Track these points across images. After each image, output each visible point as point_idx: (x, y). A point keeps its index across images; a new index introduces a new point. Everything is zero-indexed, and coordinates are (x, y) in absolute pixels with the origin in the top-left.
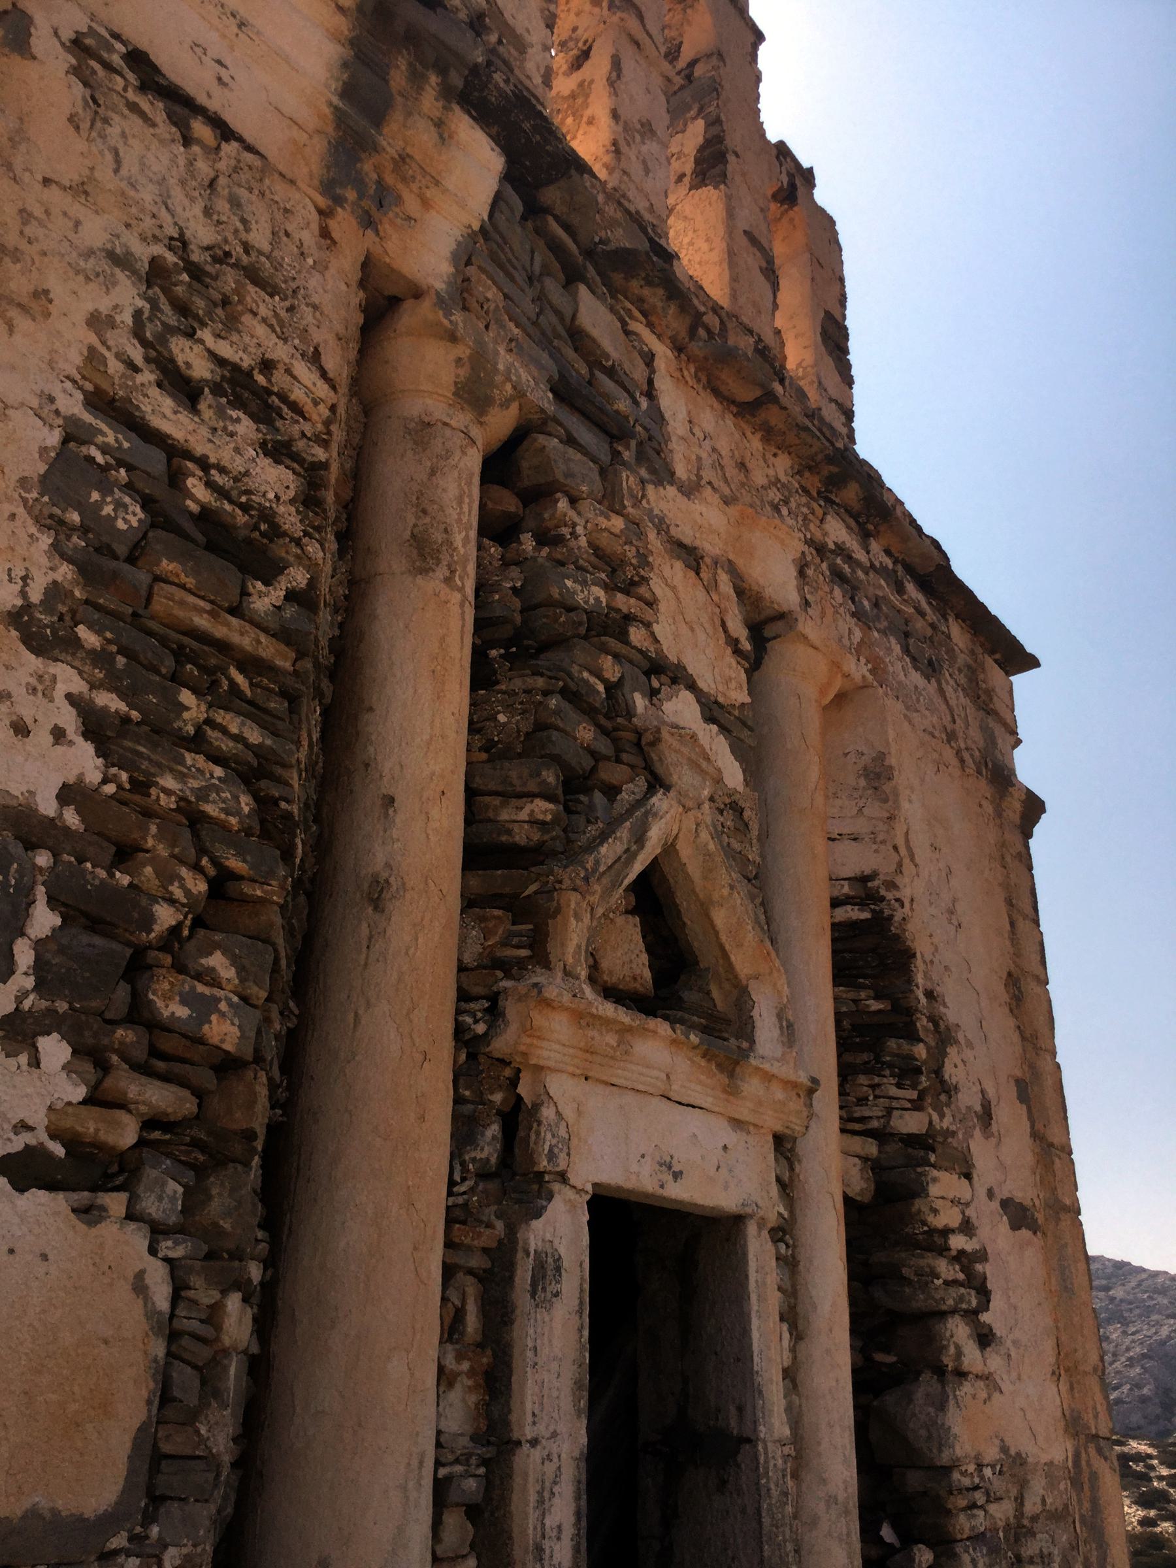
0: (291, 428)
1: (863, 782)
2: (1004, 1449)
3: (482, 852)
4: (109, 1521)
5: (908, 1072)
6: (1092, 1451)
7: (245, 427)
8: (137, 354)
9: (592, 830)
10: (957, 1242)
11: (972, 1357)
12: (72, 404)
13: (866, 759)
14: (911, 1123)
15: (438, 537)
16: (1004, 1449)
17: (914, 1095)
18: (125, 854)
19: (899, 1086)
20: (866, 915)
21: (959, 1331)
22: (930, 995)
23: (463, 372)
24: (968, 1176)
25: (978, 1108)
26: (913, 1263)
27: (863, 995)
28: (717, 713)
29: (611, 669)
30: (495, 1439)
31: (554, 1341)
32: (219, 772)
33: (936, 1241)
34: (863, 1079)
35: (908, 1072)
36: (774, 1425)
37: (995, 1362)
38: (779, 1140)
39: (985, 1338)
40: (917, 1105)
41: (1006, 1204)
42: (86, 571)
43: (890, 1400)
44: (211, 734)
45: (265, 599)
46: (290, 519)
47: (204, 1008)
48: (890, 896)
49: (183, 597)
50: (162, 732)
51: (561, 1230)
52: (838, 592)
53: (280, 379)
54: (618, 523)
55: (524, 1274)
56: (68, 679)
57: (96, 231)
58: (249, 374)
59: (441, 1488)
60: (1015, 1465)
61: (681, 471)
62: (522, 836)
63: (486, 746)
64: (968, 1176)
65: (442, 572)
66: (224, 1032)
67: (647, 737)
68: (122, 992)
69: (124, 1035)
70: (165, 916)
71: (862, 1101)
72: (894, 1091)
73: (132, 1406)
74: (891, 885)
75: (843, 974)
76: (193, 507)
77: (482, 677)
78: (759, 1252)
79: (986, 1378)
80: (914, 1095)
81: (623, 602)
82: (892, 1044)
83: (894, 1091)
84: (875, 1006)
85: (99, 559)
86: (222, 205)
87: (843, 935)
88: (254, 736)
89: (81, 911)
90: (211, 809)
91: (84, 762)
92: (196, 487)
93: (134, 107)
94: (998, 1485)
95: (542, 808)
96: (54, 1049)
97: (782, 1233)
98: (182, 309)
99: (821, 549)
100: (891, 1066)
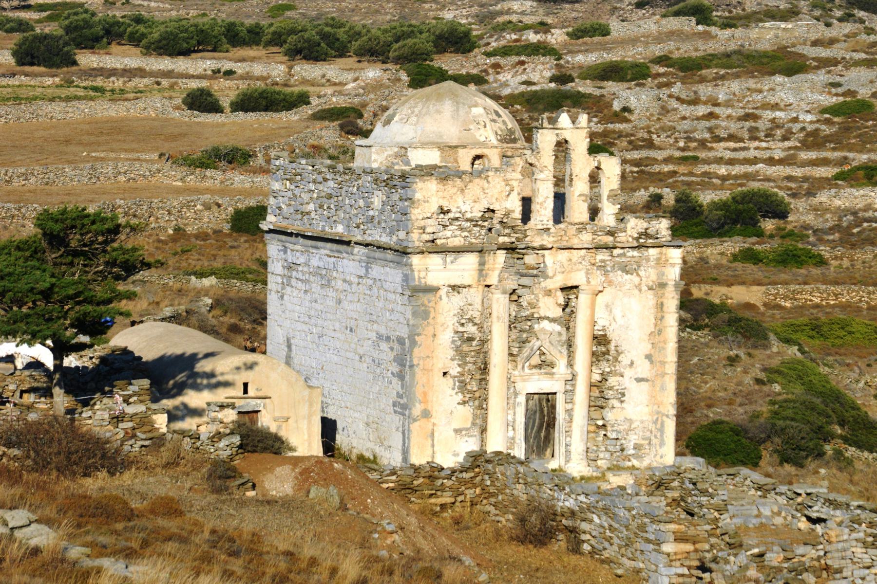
0: (477, 321)
3: (511, 355)
7: (471, 324)
12: (452, 335)
14: (608, 370)
29: (529, 323)
31: (521, 412)
33: (611, 388)
35: (608, 360)
37: (624, 405)
41: (636, 379)
42: (456, 351)
45: (474, 343)
46: (477, 332)
49: (465, 348)
50: (466, 363)
51: (522, 399)
52: (598, 272)
54: (533, 297)
56: (456, 362)
57: (452, 314)
59: (508, 425)
61: (550, 274)
62: (515, 353)
66: (475, 389)
73: (471, 419)
81: (533, 310)
85: (457, 349)
89: (461, 382)
91: (459, 369)
92: (466, 335)
99: (594, 264)
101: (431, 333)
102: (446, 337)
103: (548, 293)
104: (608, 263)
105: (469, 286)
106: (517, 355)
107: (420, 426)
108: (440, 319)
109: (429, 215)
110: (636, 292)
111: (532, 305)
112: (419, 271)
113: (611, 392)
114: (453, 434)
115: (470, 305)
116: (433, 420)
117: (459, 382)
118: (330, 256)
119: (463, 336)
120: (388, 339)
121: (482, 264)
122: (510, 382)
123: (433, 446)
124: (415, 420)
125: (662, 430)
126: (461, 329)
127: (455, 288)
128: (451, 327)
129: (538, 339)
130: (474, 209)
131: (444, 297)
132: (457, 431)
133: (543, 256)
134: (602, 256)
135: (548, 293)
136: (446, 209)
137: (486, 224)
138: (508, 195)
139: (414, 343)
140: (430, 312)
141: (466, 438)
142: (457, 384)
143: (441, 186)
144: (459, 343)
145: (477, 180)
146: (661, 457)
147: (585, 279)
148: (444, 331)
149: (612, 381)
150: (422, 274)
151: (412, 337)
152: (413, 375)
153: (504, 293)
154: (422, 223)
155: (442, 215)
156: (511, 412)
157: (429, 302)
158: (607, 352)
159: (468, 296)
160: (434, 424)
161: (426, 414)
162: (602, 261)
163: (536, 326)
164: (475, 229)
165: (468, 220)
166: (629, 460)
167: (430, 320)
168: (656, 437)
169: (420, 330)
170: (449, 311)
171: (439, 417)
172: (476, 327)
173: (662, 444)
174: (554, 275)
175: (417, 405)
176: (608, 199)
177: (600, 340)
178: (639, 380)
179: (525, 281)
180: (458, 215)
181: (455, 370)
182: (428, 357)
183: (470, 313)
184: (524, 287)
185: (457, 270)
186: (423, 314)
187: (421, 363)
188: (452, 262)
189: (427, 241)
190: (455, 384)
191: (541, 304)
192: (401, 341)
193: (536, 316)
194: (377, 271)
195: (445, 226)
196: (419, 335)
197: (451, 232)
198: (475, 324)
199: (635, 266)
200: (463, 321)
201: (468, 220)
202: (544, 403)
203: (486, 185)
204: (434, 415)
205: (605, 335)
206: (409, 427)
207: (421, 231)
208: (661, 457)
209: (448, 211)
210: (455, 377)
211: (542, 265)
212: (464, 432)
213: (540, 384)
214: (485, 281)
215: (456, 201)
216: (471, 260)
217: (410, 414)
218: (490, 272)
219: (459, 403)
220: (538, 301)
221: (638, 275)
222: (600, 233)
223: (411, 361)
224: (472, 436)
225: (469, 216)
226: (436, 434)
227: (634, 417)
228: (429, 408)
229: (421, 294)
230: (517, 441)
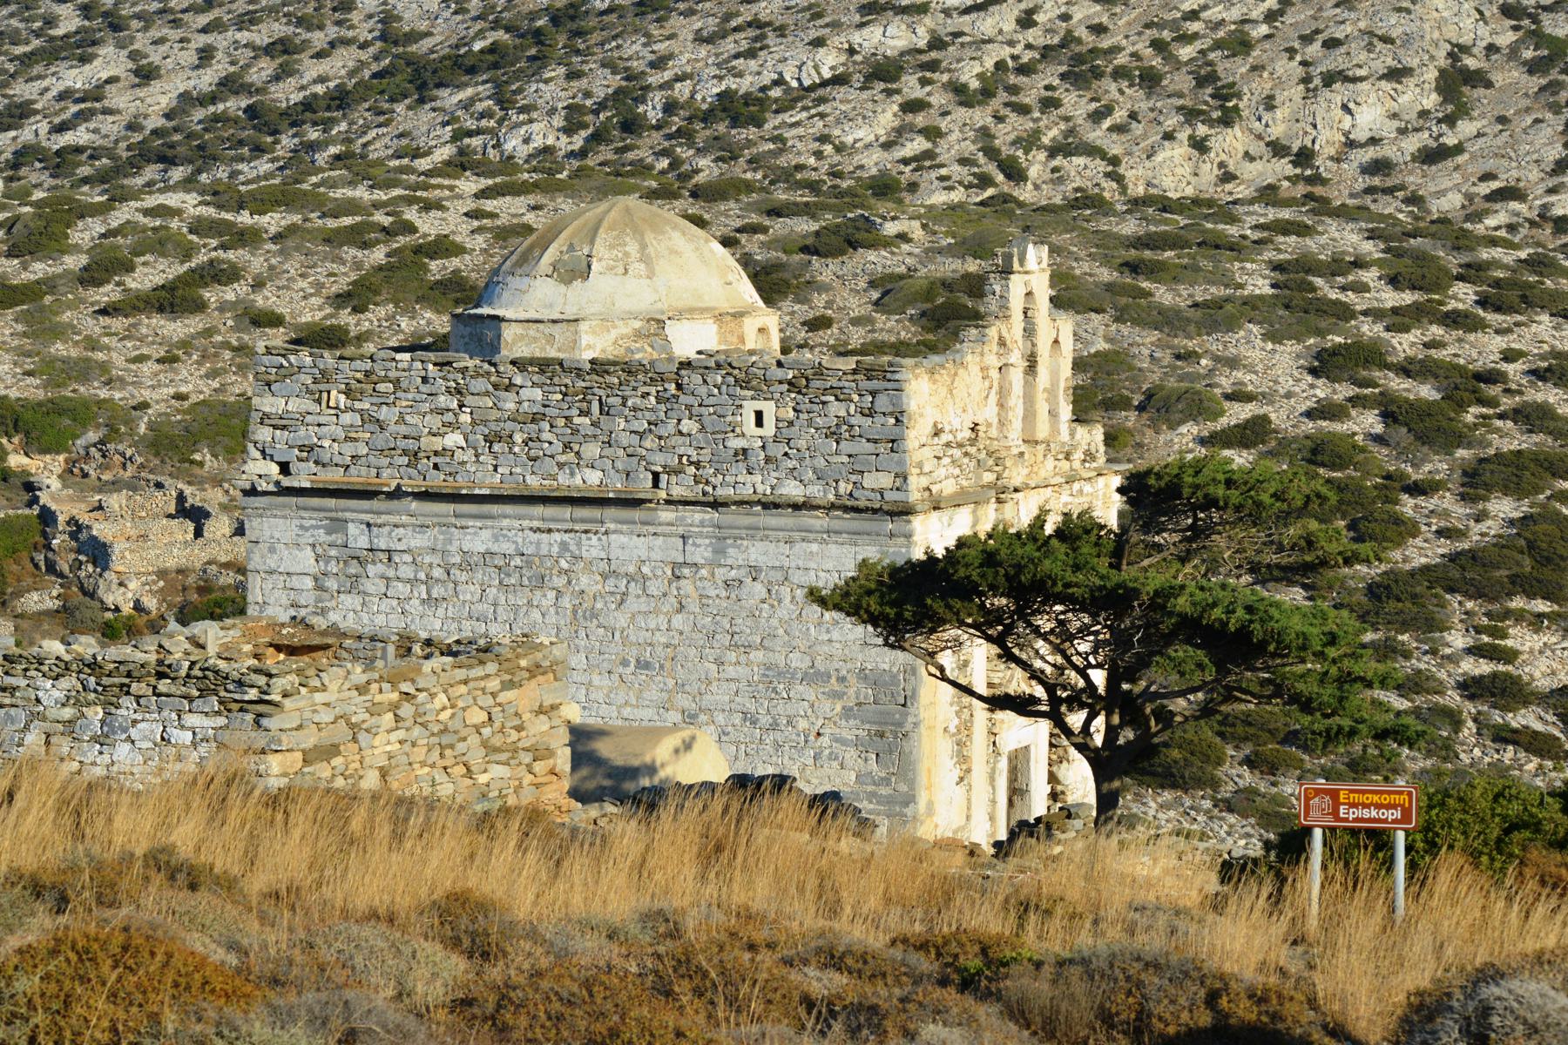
118: (550, 531)
194: (757, 553)
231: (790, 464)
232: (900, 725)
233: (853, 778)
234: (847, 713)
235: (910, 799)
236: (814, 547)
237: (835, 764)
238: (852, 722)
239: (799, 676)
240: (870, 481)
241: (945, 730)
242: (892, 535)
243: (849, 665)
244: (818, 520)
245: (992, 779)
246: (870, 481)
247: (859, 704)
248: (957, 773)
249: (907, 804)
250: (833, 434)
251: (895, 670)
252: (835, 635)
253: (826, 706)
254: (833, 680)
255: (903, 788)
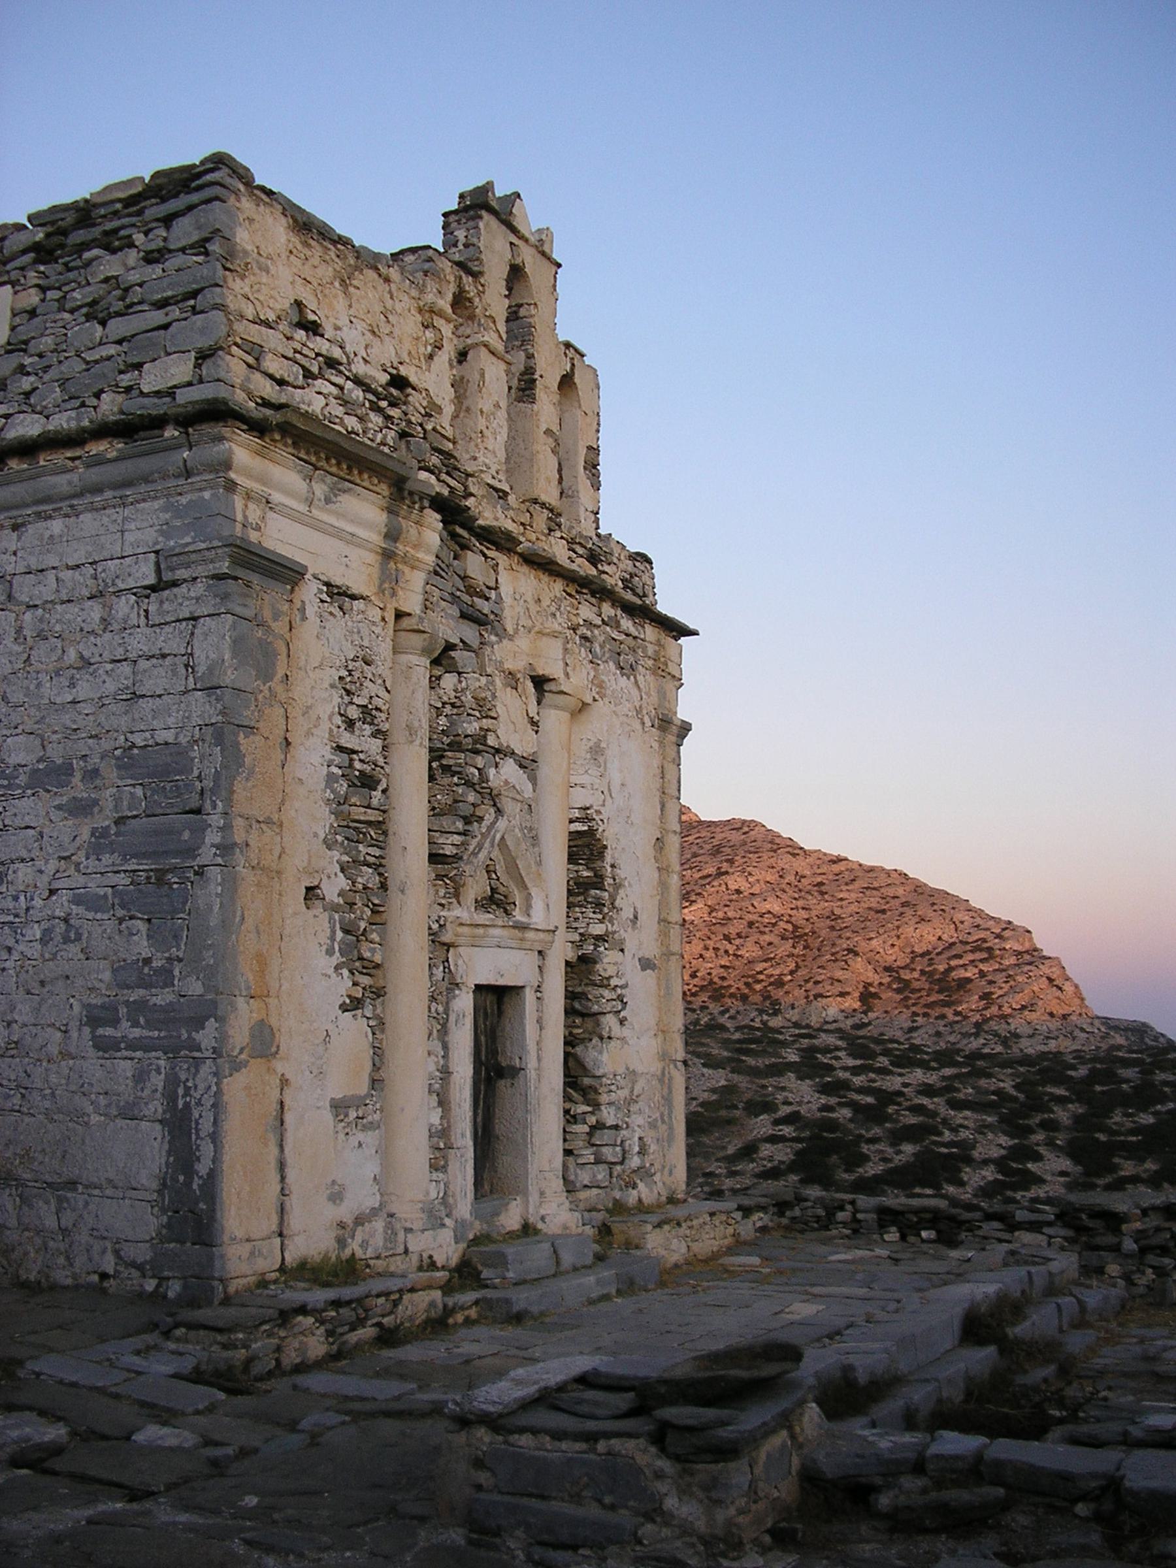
1: (588, 756)
2: (628, 1069)
3: (435, 858)
4: (366, 1096)
5: (599, 905)
6: (672, 1066)
8: (338, 720)
9: (474, 842)
10: (613, 982)
11: (616, 1030)
13: (591, 744)
14: (598, 929)
15: (416, 724)
16: (628, 1069)
17: (600, 917)
18: (352, 904)
19: (594, 912)
20: (586, 828)
21: (610, 1021)
22: (613, 866)
23: (426, 644)
24: (622, 950)
25: (631, 917)
26: (593, 992)
27: (581, 868)
28: (524, 762)
29: (480, 761)
30: (446, 1072)
31: (463, 1038)
32: (370, 870)
33: (604, 983)
34: (577, 909)
35: (599, 905)
36: (531, 1063)
37: (626, 1032)
38: (540, 952)
39: (622, 1022)
40: (601, 921)
42: (337, 814)
43: (579, 1050)
44: (368, 858)
47: (373, 951)
48: (597, 818)
51: (464, 1002)
53: (376, 701)
54: (484, 680)
55: (452, 1018)
56: (336, 855)
58: (366, 706)
60: (632, 1074)
63: (435, 812)
64: (622, 950)
65: (418, 742)
67: (495, 792)
68: (356, 952)
69: (357, 964)
70: (363, 925)
71: (576, 919)
72: (591, 915)
73: (368, 1066)
74: (598, 812)
75: (572, 858)
76: (357, 773)
77: (432, 778)
78: (529, 996)
79: (623, 1039)
80: (600, 917)
81: (486, 723)
82: (593, 892)
83: (591, 915)
84: (586, 874)
86: (356, 637)
87: (574, 836)
88: (377, 852)
90: (370, 885)
91: (342, 882)
92: (358, 765)
93: (331, 613)
94: (622, 1083)
95: (457, 839)
96: (345, 972)
97: (538, 989)
98: (348, 692)
100: (591, 903)
101: (280, 732)
102: (313, 759)
103: (512, 679)
104: (596, 632)
105: (362, 598)
106: (457, 858)
107: (247, 1088)
108: (301, 690)
109: (272, 317)
110: (637, 725)
111: (484, 708)
112: (248, 496)
113: (607, 994)
114: (328, 1116)
115: (368, 663)
116: (280, 1066)
117: (347, 932)
119: (351, 766)
120: (49, 776)
121: (392, 535)
122: (440, 945)
123: (282, 1166)
124: (237, 1067)
125: (668, 1100)
126: (347, 740)
127: (337, 594)
128: (325, 725)
129: (499, 812)
130: (374, 351)
131: (311, 611)
132: (339, 1107)
133: (495, 568)
134: (586, 612)
135: (512, 679)
136: (312, 317)
137: (394, 412)
138: (431, 357)
139: (234, 759)
140: (276, 654)
141: (361, 1136)
142: (339, 935)
143: (295, 240)
144: (342, 787)
145: (371, 274)
146: (671, 1173)
147: (561, 663)
148: (309, 734)
149: (609, 962)
150: (254, 513)
151: (225, 733)
152: (231, 884)
153: (425, 651)
154: (256, 333)
155: (301, 334)
156: (437, 1046)
157: (276, 618)
158: (598, 882)
159: (365, 632)
160: (284, 1082)
161: (265, 1043)
162: (588, 623)
163: (492, 771)
164: (372, 415)
165: (358, 381)
166: (634, 1186)
167: (276, 684)
168: (663, 1122)
169: (247, 715)
170: (320, 667)
171: (295, 1059)
172: (379, 742)
173: (671, 1138)
174: (516, 631)
175: (241, 1002)
176: (585, 468)
177: (585, 847)
178: (646, 964)
179: (470, 633)
180: (337, 353)
181: (334, 886)
182: (268, 821)
183: (371, 688)
184: (467, 646)
185: (337, 534)
186: (263, 655)
187: (253, 840)
188: (328, 501)
189: (266, 403)
190: (332, 938)
191: (500, 709)
192: (157, 767)
193: (491, 741)
195: (308, 374)
196: (251, 729)
197: (321, 401)
198: (377, 734)
199: (631, 659)
200: (354, 713)
201: (358, 381)
202: (481, 1020)
203: (389, 303)
204: (283, 1040)
205: (591, 832)
206: (219, 1093)
207: (250, 360)
208: (671, 1173)
209: (313, 328)
210: (335, 908)
211: (493, 594)
212: (353, 1114)
213: (487, 962)
214: (394, 594)
215: (331, 307)
216: (364, 510)
217: (222, 1038)
218: (407, 570)
219: (344, 1008)
220: (494, 696)
221: (636, 682)
222: (580, 551)
223: (226, 828)
224: (372, 1126)
225: (359, 368)
226: (289, 1118)
227: (640, 1069)
228: (273, 1022)
229: (255, 579)
230: (459, 1143)
231: (27, 383)
232: (191, 852)
233: (107, 976)
234: (100, 843)
235: (206, 1011)
236: (56, 526)
237: (74, 949)
238: (107, 859)
239: (22, 779)
240: (152, 379)
241: (311, 892)
242: (188, 473)
243: (106, 745)
244: (60, 474)
245: (442, 1029)
246: (152, 379)
247: (120, 821)
248: (342, 986)
249: (198, 1023)
250: (96, 313)
251: (183, 740)
252: (84, 690)
253: (64, 828)
254: (76, 779)
255: (195, 988)
